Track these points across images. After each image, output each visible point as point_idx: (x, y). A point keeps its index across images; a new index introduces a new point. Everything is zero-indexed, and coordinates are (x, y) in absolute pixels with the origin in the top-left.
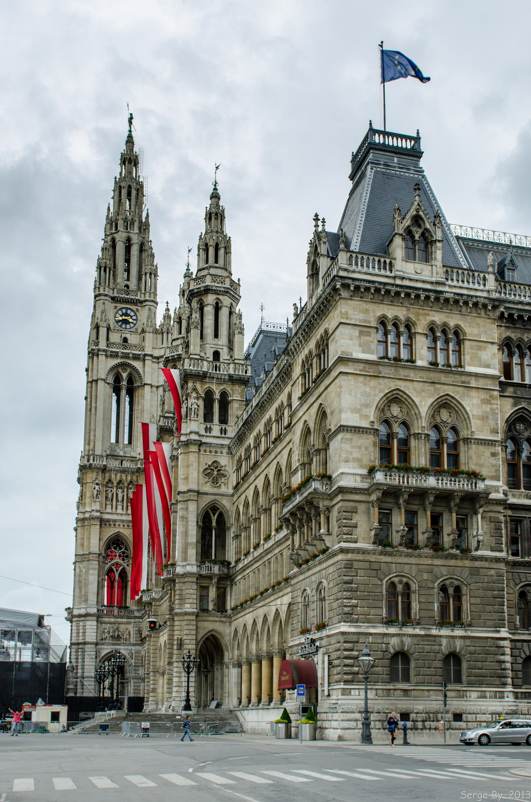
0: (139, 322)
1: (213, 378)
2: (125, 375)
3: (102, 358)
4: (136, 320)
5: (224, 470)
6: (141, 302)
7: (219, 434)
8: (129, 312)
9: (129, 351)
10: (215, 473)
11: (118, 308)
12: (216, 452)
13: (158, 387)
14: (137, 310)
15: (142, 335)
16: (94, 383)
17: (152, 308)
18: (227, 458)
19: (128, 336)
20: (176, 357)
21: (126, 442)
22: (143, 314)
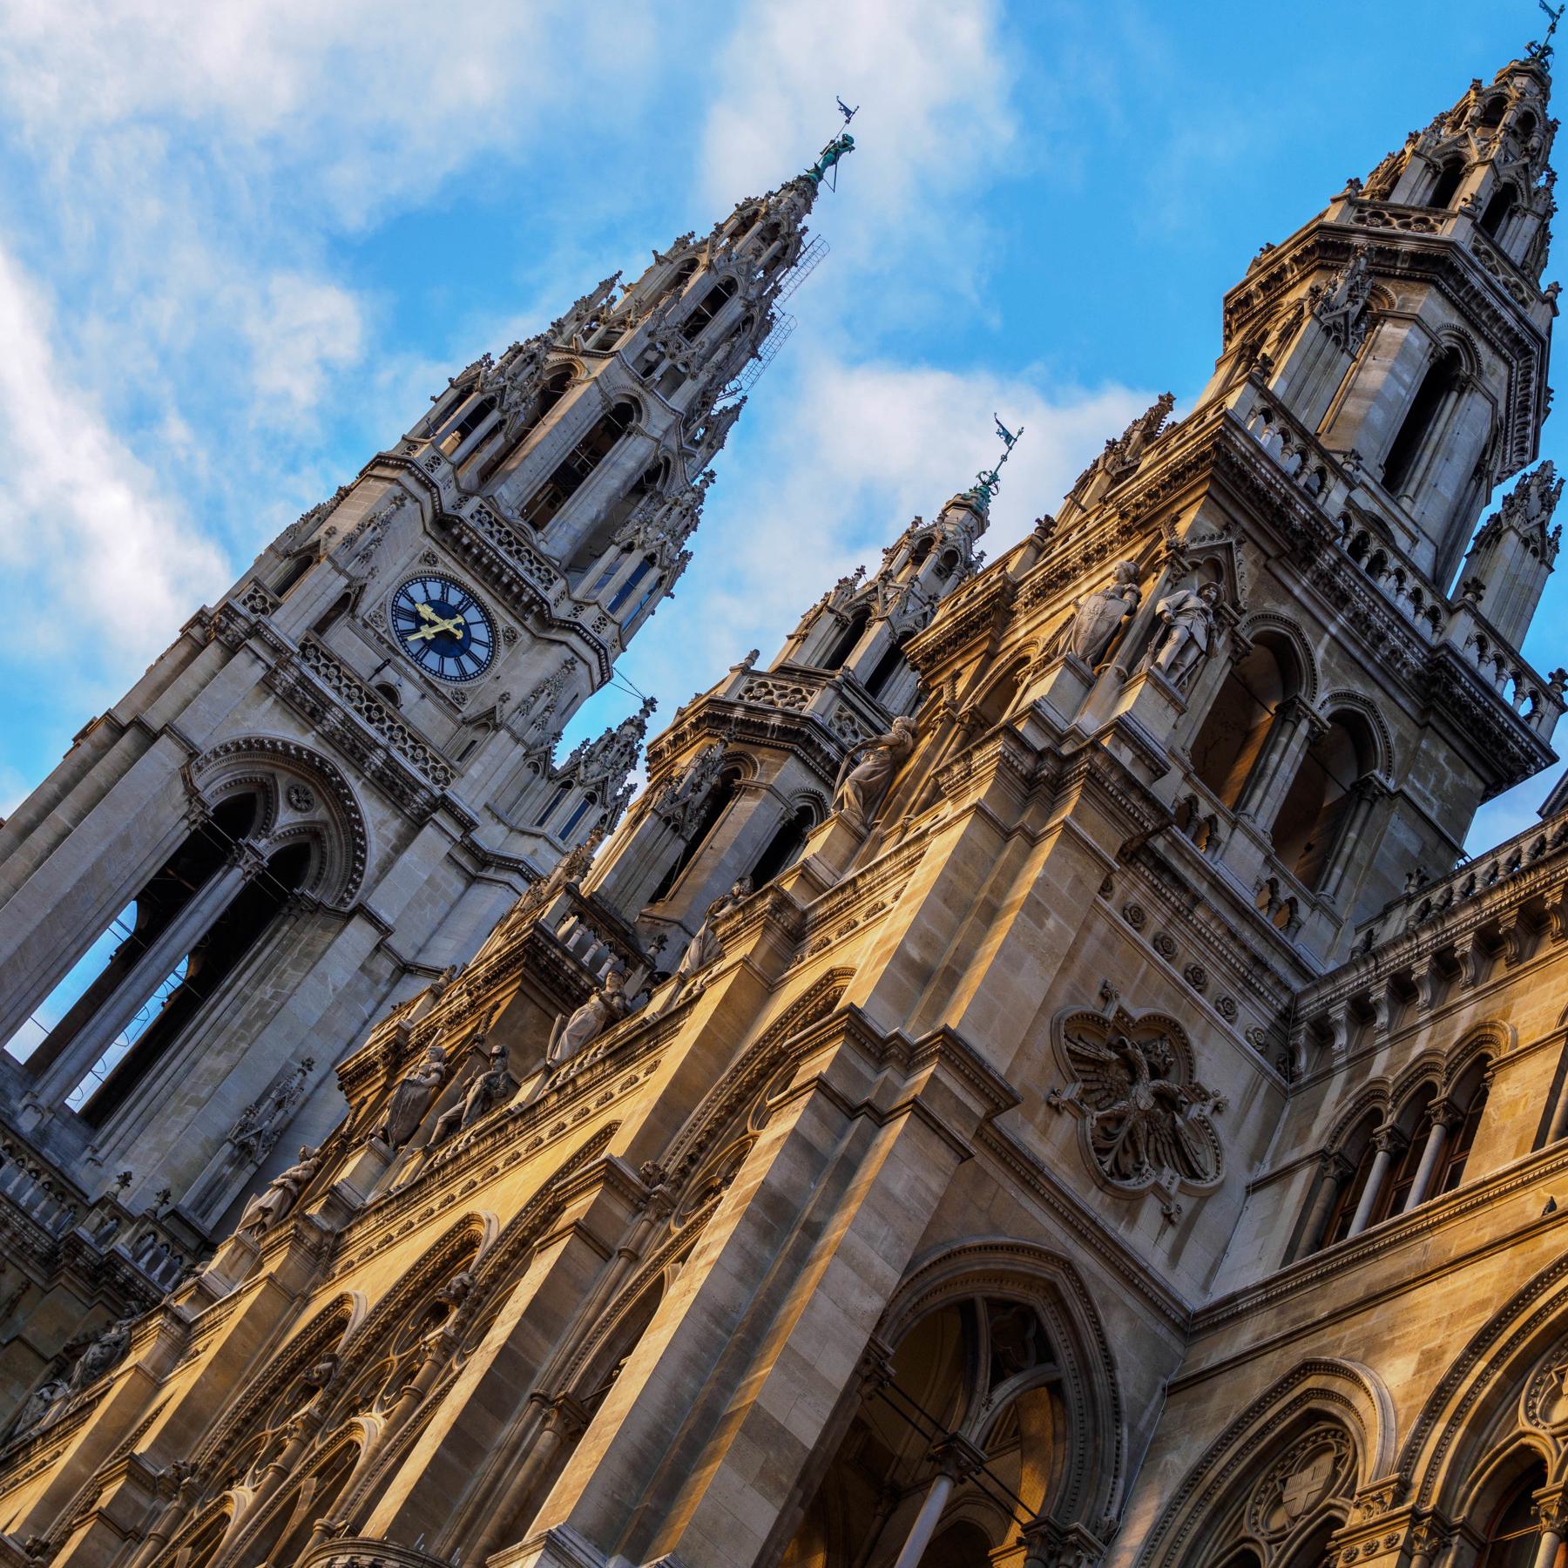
0: (485, 680)
1: (1342, 600)
2: (286, 818)
3: (247, 670)
4: (483, 666)
5: (1204, 1124)
6: (546, 621)
7: (1250, 899)
8: (473, 614)
9: (383, 741)
10: (1142, 1095)
11: (439, 568)
12: (1196, 977)
13: (405, 969)
14: (512, 638)
15: (470, 734)
16: (126, 742)
17: (581, 668)
18: (1247, 1071)
19: (409, 693)
20: (775, 720)
21: (77, 1100)
22: (525, 668)
